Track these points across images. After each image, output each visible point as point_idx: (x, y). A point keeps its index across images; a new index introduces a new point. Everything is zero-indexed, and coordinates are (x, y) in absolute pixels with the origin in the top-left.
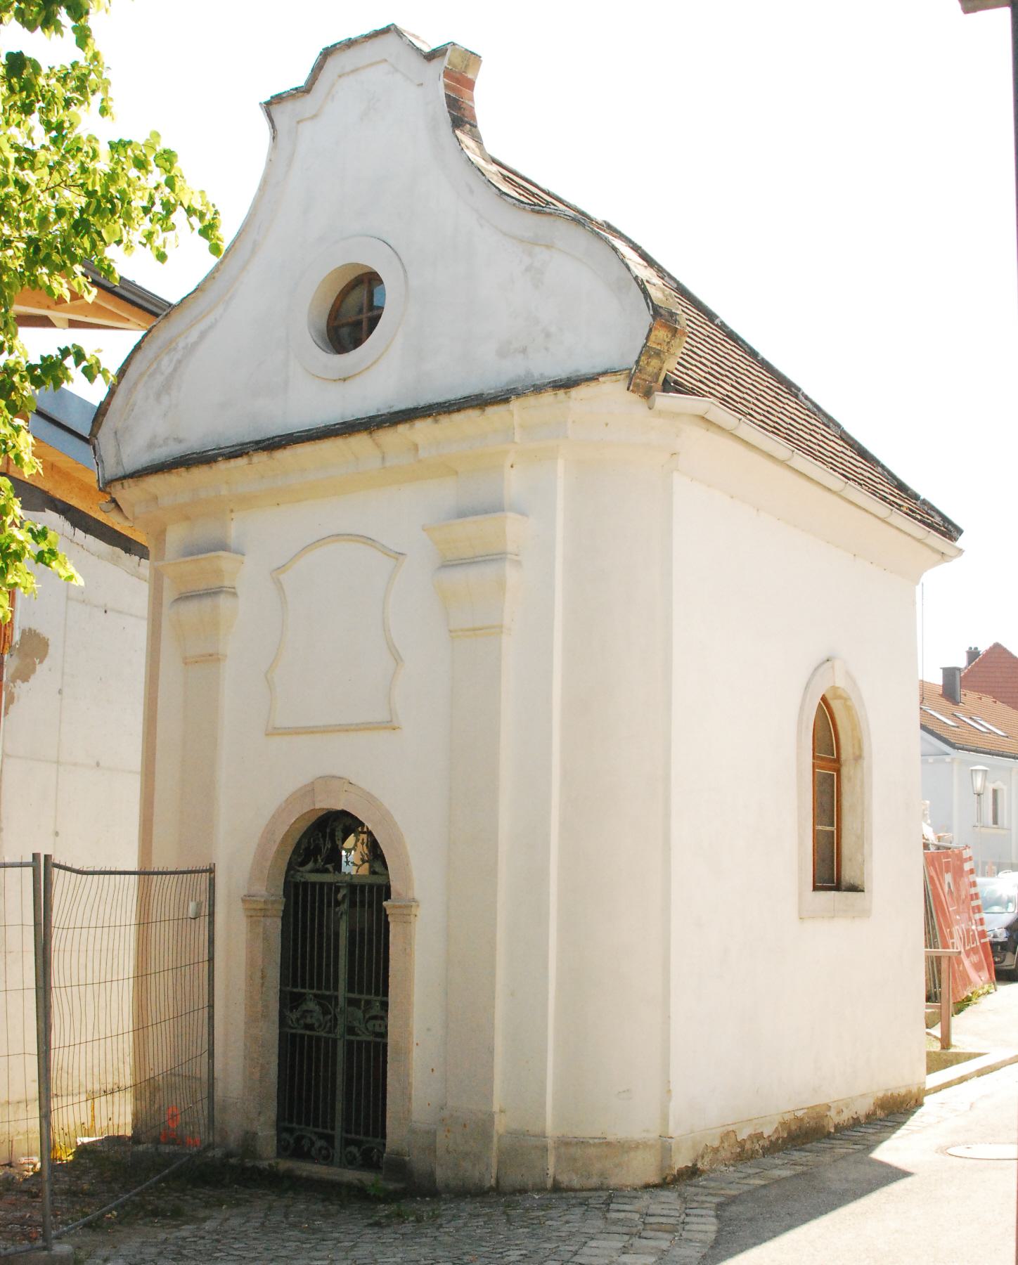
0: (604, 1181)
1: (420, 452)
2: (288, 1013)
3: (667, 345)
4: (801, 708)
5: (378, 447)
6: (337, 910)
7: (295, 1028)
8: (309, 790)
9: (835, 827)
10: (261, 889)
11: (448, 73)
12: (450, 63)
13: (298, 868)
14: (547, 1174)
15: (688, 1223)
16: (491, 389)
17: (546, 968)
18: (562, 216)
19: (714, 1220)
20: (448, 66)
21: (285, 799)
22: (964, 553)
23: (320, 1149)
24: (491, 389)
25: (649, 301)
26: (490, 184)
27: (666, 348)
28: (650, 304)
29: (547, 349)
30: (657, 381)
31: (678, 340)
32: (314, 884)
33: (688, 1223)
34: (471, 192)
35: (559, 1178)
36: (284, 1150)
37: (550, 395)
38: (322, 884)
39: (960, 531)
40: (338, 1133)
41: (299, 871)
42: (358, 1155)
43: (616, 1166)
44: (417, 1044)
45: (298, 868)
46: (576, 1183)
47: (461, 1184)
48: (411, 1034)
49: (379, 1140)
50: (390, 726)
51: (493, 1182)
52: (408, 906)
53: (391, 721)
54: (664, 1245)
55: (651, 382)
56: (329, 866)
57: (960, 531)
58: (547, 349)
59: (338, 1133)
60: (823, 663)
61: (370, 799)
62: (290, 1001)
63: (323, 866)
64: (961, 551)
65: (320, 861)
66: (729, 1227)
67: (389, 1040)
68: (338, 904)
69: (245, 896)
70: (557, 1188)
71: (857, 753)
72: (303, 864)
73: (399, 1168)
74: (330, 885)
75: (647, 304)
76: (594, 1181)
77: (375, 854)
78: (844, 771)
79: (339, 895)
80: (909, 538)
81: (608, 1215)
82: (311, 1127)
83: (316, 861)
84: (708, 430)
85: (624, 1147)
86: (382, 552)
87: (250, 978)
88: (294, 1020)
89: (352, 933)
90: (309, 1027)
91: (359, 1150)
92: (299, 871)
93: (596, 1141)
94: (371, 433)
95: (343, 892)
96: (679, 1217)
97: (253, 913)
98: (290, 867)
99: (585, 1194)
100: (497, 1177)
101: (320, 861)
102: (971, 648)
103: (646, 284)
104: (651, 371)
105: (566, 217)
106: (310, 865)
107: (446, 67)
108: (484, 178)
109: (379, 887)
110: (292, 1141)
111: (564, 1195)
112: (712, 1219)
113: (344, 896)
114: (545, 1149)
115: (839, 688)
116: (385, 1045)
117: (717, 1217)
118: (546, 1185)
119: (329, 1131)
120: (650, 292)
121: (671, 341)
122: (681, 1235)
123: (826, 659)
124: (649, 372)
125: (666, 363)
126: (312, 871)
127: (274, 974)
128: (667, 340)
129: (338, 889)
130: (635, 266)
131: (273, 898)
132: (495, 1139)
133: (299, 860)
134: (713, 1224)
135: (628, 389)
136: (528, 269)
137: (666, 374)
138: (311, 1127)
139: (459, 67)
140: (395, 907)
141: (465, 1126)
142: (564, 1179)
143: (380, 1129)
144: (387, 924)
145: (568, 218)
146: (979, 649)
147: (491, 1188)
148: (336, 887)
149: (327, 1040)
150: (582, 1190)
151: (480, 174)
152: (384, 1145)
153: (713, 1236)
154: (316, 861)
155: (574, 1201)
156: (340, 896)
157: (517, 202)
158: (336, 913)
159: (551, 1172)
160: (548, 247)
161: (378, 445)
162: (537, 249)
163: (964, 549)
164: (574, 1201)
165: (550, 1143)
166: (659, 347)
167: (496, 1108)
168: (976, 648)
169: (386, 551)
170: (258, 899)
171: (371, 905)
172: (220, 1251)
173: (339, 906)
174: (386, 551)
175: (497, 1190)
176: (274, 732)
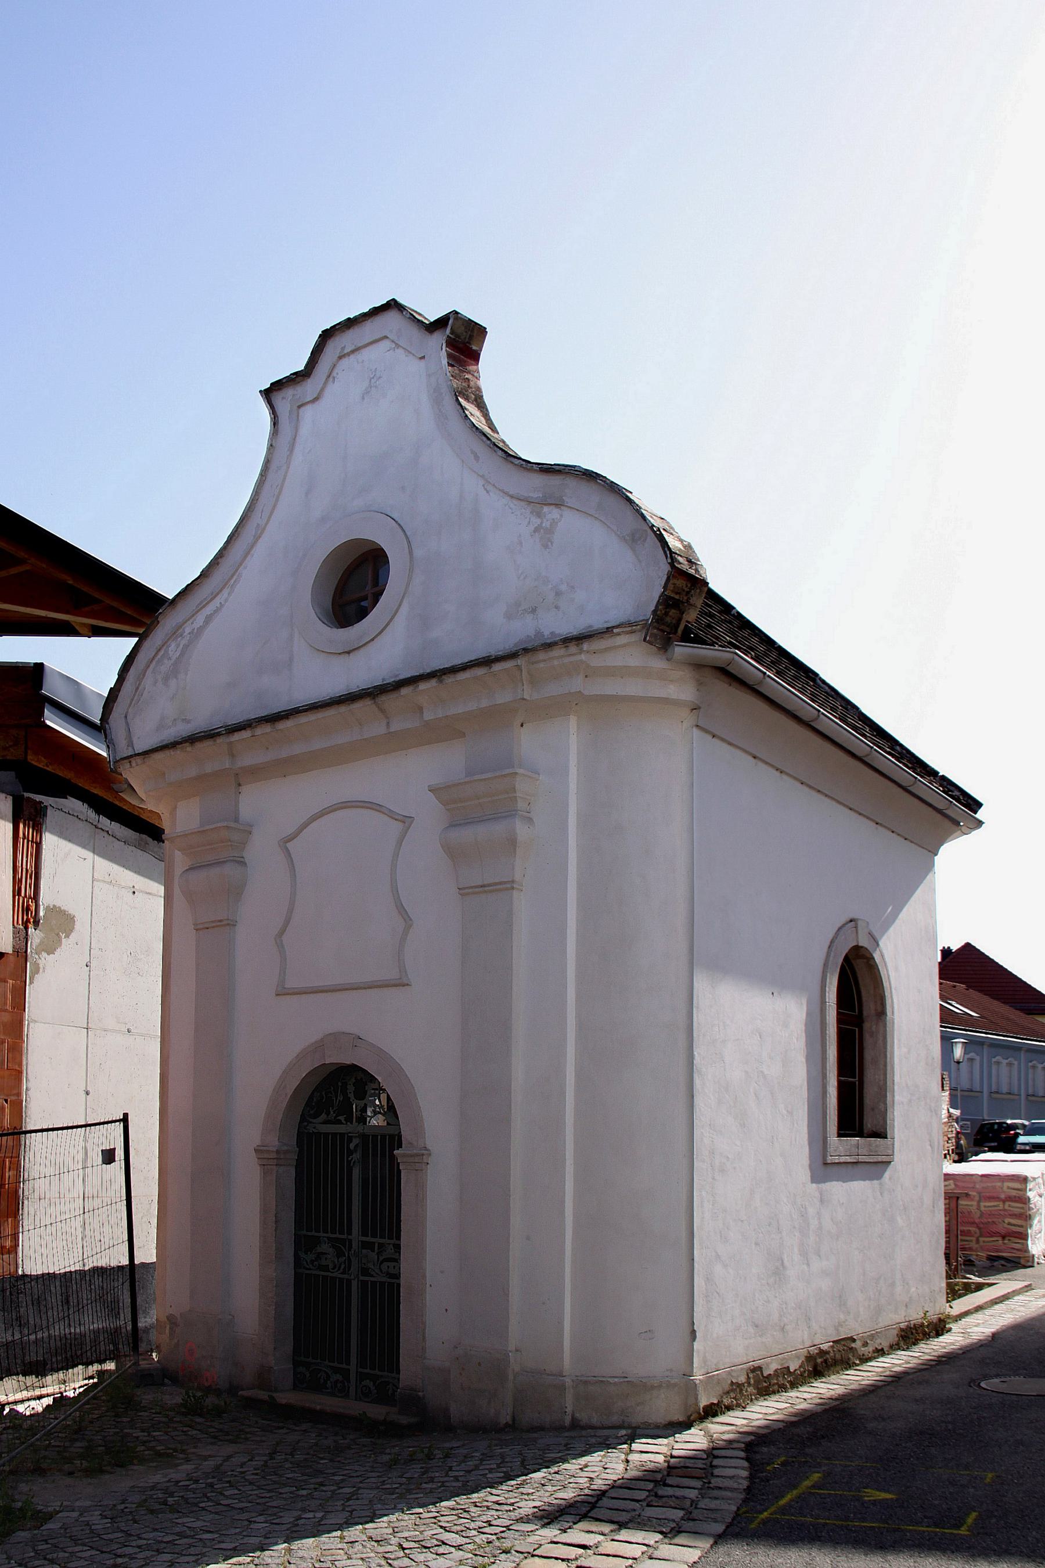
0: (626, 1418)
1: (425, 714)
2: (302, 1255)
3: (686, 595)
4: (824, 965)
5: (382, 712)
6: (350, 1159)
7: (310, 1269)
8: (320, 1046)
9: (857, 1079)
10: (274, 1142)
11: (451, 343)
12: (452, 332)
13: (311, 1120)
14: (566, 1412)
15: (716, 1467)
16: (499, 651)
17: (562, 1213)
18: (572, 472)
19: (746, 1464)
20: (450, 335)
21: (295, 1055)
22: (983, 825)
23: (337, 1381)
24: (499, 651)
25: (666, 549)
26: (496, 448)
27: (685, 598)
28: (668, 552)
29: (557, 607)
30: (675, 633)
31: (698, 591)
32: (326, 1135)
33: (716, 1467)
34: (477, 458)
35: (577, 1415)
36: (299, 1384)
37: (561, 648)
38: (334, 1135)
39: (979, 805)
40: (353, 1367)
41: (311, 1122)
42: (373, 1388)
43: (638, 1404)
44: (431, 1286)
45: (311, 1120)
46: (595, 1421)
47: (477, 1420)
48: (424, 1276)
49: (394, 1375)
50: (401, 984)
51: (509, 1419)
52: (421, 1157)
53: (400, 978)
54: (693, 1494)
55: (669, 633)
56: (342, 1118)
57: (979, 805)
58: (557, 607)
59: (353, 1367)
60: (847, 923)
61: (382, 1055)
62: (303, 1244)
63: (335, 1117)
64: (980, 823)
65: (332, 1113)
66: (762, 1473)
67: (402, 1281)
68: (350, 1153)
69: (258, 1146)
70: (576, 1425)
71: (880, 1009)
72: (316, 1116)
73: (413, 1402)
74: (342, 1135)
75: (665, 552)
76: (615, 1419)
77: (391, 1110)
78: (866, 1026)
79: (351, 1145)
80: (930, 809)
81: (631, 1457)
82: (327, 1362)
83: (328, 1114)
84: (730, 685)
85: (644, 1387)
86: (388, 816)
87: (264, 1223)
88: (308, 1261)
89: (365, 1182)
90: (322, 1268)
91: (374, 1384)
92: (311, 1122)
93: (616, 1380)
94: (374, 698)
95: (355, 1141)
96: (706, 1459)
97: (265, 1162)
98: (303, 1118)
99: (606, 1432)
100: (513, 1413)
101: (332, 1113)
102: (944, 948)
103: (663, 532)
104: (669, 621)
105: (576, 473)
106: (323, 1116)
107: (448, 336)
108: (489, 442)
109: (392, 1137)
110: (308, 1375)
111: (584, 1433)
112: (742, 1461)
113: (357, 1146)
114: (562, 1388)
115: (862, 947)
116: (399, 1285)
117: (747, 1459)
118: (564, 1422)
119: (344, 1366)
120: (667, 540)
121: (690, 591)
122: (710, 1483)
123: (849, 920)
124: (667, 622)
125: (685, 613)
126: (325, 1122)
127: (289, 1218)
128: (686, 589)
129: (350, 1139)
130: (651, 517)
131: (285, 1148)
132: (511, 1377)
133: (312, 1112)
134: (743, 1468)
135: (645, 640)
136: (537, 530)
137: (686, 625)
138: (327, 1362)
139: (462, 337)
140: (404, 1155)
141: (479, 1364)
142: (583, 1417)
143: (394, 1366)
144: (399, 1172)
145: (578, 473)
146: (951, 948)
147: (507, 1425)
148: (348, 1136)
149: (341, 1280)
150: (603, 1428)
151: (485, 439)
152: (399, 1379)
153: (745, 1484)
154: (328, 1114)
155: (593, 1440)
156: (352, 1146)
157: (524, 463)
158: (349, 1162)
159: (569, 1410)
160: (557, 505)
161: (382, 711)
162: (546, 509)
163: (983, 821)
164: (593, 1440)
165: (568, 1381)
166: (677, 597)
167: (512, 1346)
168: (949, 948)
169: (392, 815)
170: (271, 1149)
171: (383, 1155)
172: (209, 1499)
173: (352, 1155)
174: (392, 815)
175: (513, 1426)
176: (282, 992)
